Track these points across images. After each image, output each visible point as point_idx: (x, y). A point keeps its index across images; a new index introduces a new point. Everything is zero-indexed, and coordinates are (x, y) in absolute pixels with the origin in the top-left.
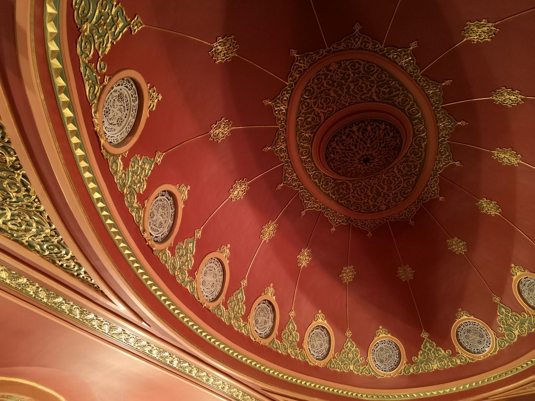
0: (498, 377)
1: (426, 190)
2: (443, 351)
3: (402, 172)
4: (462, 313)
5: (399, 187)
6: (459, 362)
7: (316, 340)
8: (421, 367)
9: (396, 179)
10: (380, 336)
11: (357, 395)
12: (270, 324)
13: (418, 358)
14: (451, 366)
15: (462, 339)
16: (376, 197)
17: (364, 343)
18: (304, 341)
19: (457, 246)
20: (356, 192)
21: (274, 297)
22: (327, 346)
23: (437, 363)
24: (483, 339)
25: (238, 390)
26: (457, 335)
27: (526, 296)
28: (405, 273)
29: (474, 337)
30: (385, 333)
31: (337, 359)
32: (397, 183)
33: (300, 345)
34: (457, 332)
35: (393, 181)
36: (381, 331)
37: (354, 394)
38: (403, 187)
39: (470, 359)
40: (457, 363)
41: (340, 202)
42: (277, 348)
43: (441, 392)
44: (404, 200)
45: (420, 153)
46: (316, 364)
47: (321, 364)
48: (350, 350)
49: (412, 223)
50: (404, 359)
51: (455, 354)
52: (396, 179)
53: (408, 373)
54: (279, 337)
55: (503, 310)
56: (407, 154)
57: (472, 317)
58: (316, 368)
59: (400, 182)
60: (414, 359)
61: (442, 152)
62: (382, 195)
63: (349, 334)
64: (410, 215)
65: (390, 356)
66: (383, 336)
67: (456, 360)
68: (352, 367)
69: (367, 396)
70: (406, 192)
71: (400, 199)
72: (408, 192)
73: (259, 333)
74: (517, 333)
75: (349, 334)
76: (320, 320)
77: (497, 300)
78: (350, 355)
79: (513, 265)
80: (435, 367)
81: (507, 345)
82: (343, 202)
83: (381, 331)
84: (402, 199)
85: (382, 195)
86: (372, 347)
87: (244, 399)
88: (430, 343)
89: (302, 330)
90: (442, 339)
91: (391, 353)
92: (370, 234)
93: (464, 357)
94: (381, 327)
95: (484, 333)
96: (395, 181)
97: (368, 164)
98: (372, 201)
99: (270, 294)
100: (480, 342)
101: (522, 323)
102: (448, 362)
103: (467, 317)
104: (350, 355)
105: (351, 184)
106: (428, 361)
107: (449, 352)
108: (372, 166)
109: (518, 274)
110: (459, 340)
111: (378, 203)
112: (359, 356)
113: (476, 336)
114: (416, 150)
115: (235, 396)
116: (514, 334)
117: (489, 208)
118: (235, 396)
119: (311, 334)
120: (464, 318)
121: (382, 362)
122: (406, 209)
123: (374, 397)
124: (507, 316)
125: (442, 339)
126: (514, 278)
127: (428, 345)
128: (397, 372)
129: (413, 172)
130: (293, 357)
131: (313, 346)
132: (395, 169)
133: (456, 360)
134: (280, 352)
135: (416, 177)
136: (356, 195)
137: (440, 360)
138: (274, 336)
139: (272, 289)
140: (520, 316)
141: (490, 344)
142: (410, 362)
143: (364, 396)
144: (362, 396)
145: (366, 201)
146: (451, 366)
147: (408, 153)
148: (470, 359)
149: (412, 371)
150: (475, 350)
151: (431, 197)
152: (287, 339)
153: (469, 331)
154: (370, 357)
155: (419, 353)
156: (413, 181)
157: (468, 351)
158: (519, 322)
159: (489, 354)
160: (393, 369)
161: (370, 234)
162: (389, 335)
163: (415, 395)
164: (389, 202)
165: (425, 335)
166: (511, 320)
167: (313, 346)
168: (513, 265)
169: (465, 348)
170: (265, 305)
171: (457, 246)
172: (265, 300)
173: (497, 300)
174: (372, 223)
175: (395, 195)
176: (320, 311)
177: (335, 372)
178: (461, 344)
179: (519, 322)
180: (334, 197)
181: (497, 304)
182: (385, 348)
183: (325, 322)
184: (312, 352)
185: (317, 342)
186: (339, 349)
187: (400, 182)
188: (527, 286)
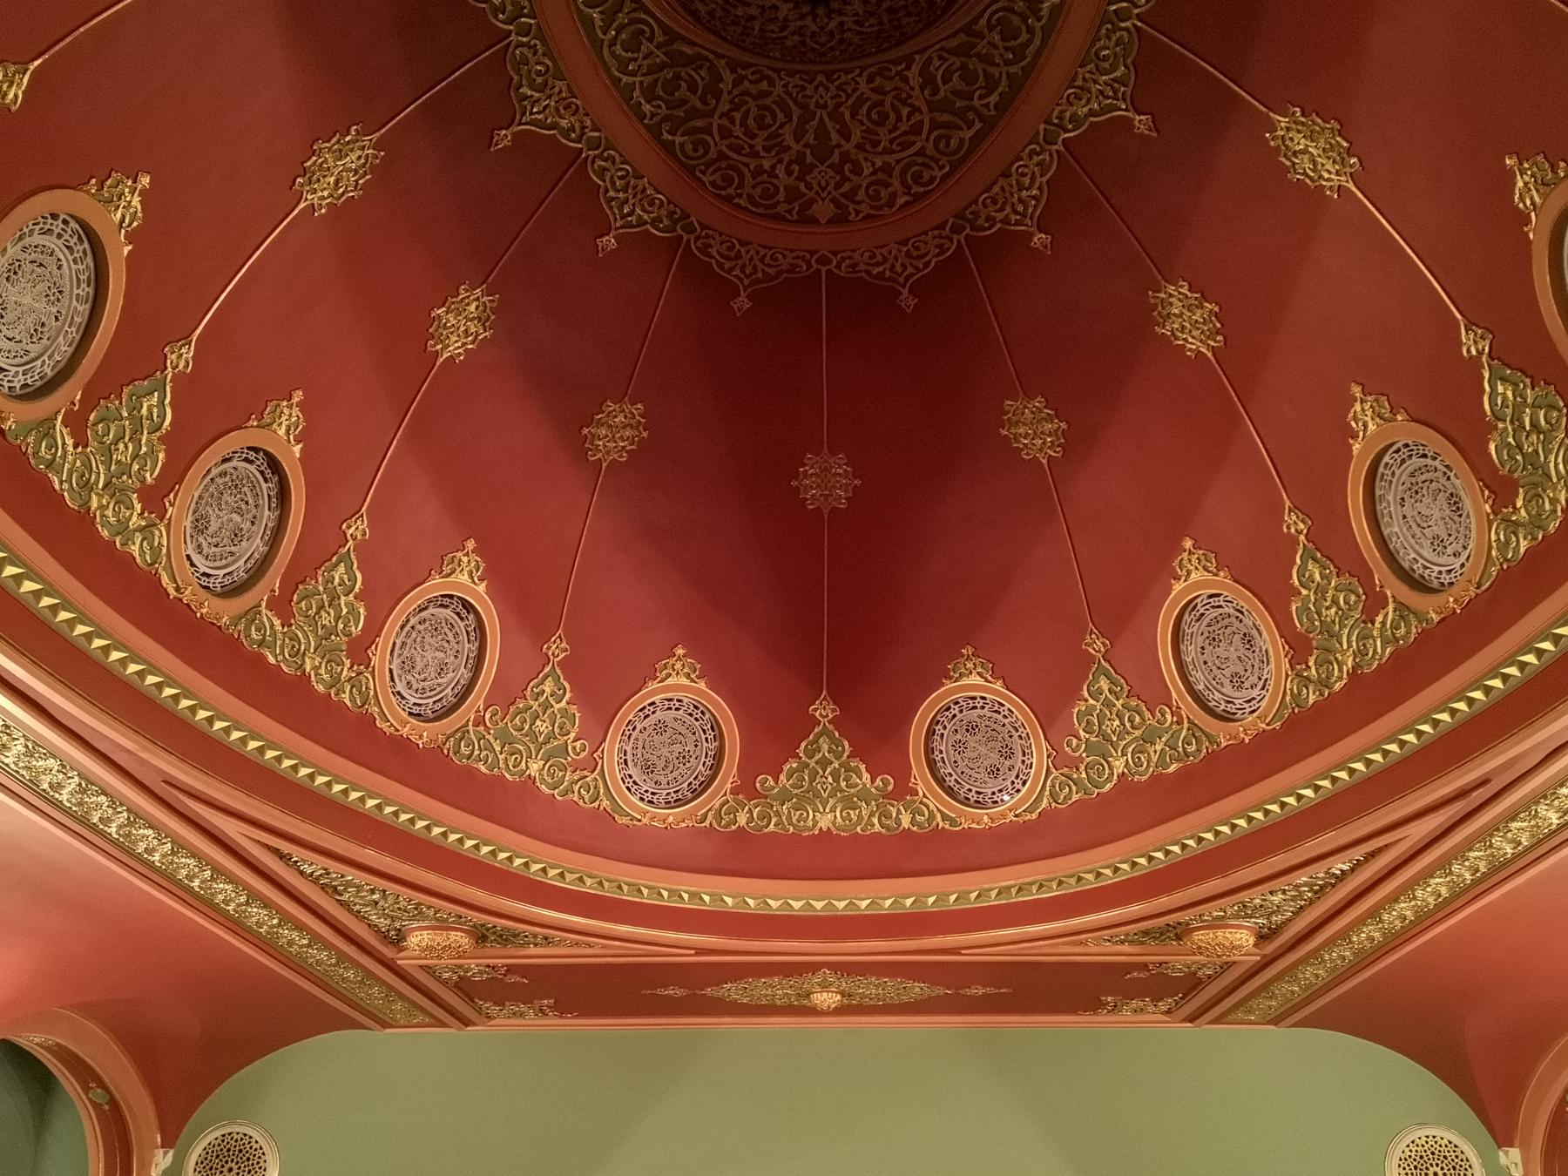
0: (1014, 891)
1: (996, 189)
2: (866, 775)
3: (935, 91)
4: (970, 665)
5: (905, 146)
6: (906, 821)
7: (425, 644)
8: (778, 814)
9: (905, 111)
10: (670, 681)
11: (526, 865)
12: (256, 546)
13: (776, 780)
14: (877, 828)
15: (942, 747)
16: (809, 159)
17: (601, 695)
18: (380, 640)
19: (1034, 430)
20: (737, 116)
21: (297, 449)
22: (464, 674)
23: (833, 810)
24: (1007, 763)
25: (63, 769)
26: (931, 733)
27: (1190, 652)
28: (827, 481)
29: (983, 750)
30: (688, 676)
31: (487, 729)
32: (903, 128)
33: (359, 651)
34: (935, 722)
35: (892, 116)
36: (678, 666)
37: (518, 862)
38: (923, 149)
39: (945, 817)
40: (899, 823)
41: (666, 136)
42: (261, 643)
43: (819, 905)
44: (907, 204)
45: (1025, 36)
46: (405, 731)
47: (423, 735)
48: (546, 706)
49: (907, 301)
50: (729, 776)
51: (902, 791)
52: (905, 111)
53: (728, 825)
54: (282, 605)
55: (1104, 684)
56: (975, 21)
57: (998, 686)
58: (402, 745)
59: (916, 130)
60: (765, 781)
61: (1105, 58)
62: (836, 158)
63: (557, 648)
64: (910, 270)
65: (683, 758)
66: (680, 682)
67: (899, 812)
68: (534, 767)
69: (562, 875)
70: (926, 176)
71: (893, 196)
72: (932, 179)
73: (203, 569)
74: (1119, 765)
75: (557, 648)
76: (464, 578)
77: (1096, 645)
78: (542, 727)
79: (1188, 544)
80: (824, 822)
81: (1075, 797)
82: (678, 139)
83: (678, 666)
84: (902, 200)
85: (836, 158)
86: (628, 712)
87: (80, 804)
88: (833, 740)
89: (380, 598)
90: (877, 734)
91: (691, 747)
92: (742, 302)
93: (931, 806)
94: (680, 651)
95: (1017, 745)
96: (899, 119)
97: (820, 11)
98: (789, 173)
99: (282, 432)
100: (994, 772)
101: (1148, 739)
102: (872, 815)
103: (981, 681)
104: (542, 727)
105: (728, 77)
106: (810, 797)
107: (885, 783)
108: (832, 25)
109: (1195, 576)
110: (929, 751)
111: (809, 187)
112: (572, 735)
113: (991, 748)
114: (1016, 20)
115: (45, 786)
116: (1111, 768)
117: (1188, 322)
118: (45, 786)
119: (413, 621)
120: (973, 680)
121: (648, 769)
122: (904, 243)
123: (589, 882)
124: (1108, 704)
125: (877, 734)
126: (1178, 587)
127: (826, 745)
128: (692, 813)
129: (976, 102)
130: (321, 688)
131: (408, 665)
132: (915, 68)
133: (899, 812)
134: (272, 660)
135: (978, 126)
136: (737, 130)
137: (849, 804)
138: (260, 594)
139: (296, 411)
140: (1147, 715)
141: (1024, 783)
142: (746, 789)
143: (552, 872)
144: (544, 870)
145: (766, 165)
146: (877, 828)
147: (983, 22)
148: (945, 817)
149: (742, 819)
150: (973, 797)
151: (1006, 221)
152: (313, 621)
153: (972, 728)
154: (611, 749)
155: (786, 767)
156: (962, 140)
157: (950, 791)
158: (1137, 733)
159: (1011, 816)
160: (679, 802)
161: (742, 302)
162: (702, 685)
163: (729, 900)
164: (851, 196)
165: (823, 711)
166: (1117, 722)
167: (408, 665)
168: (1188, 544)
169: (940, 782)
170: (252, 468)
171: (1034, 430)
172: (256, 450)
173: (1096, 645)
174: (762, 260)
175: (880, 176)
176: (471, 544)
177: (471, 773)
178: (932, 765)
179: (1137, 733)
180: (647, 108)
181: (1091, 659)
182: (675, 725)
183: (482, 588)
184: (400, 687)
185: (429, 655)
186: (505, 696)
187: (916, 130)
188: (1206, 621)
